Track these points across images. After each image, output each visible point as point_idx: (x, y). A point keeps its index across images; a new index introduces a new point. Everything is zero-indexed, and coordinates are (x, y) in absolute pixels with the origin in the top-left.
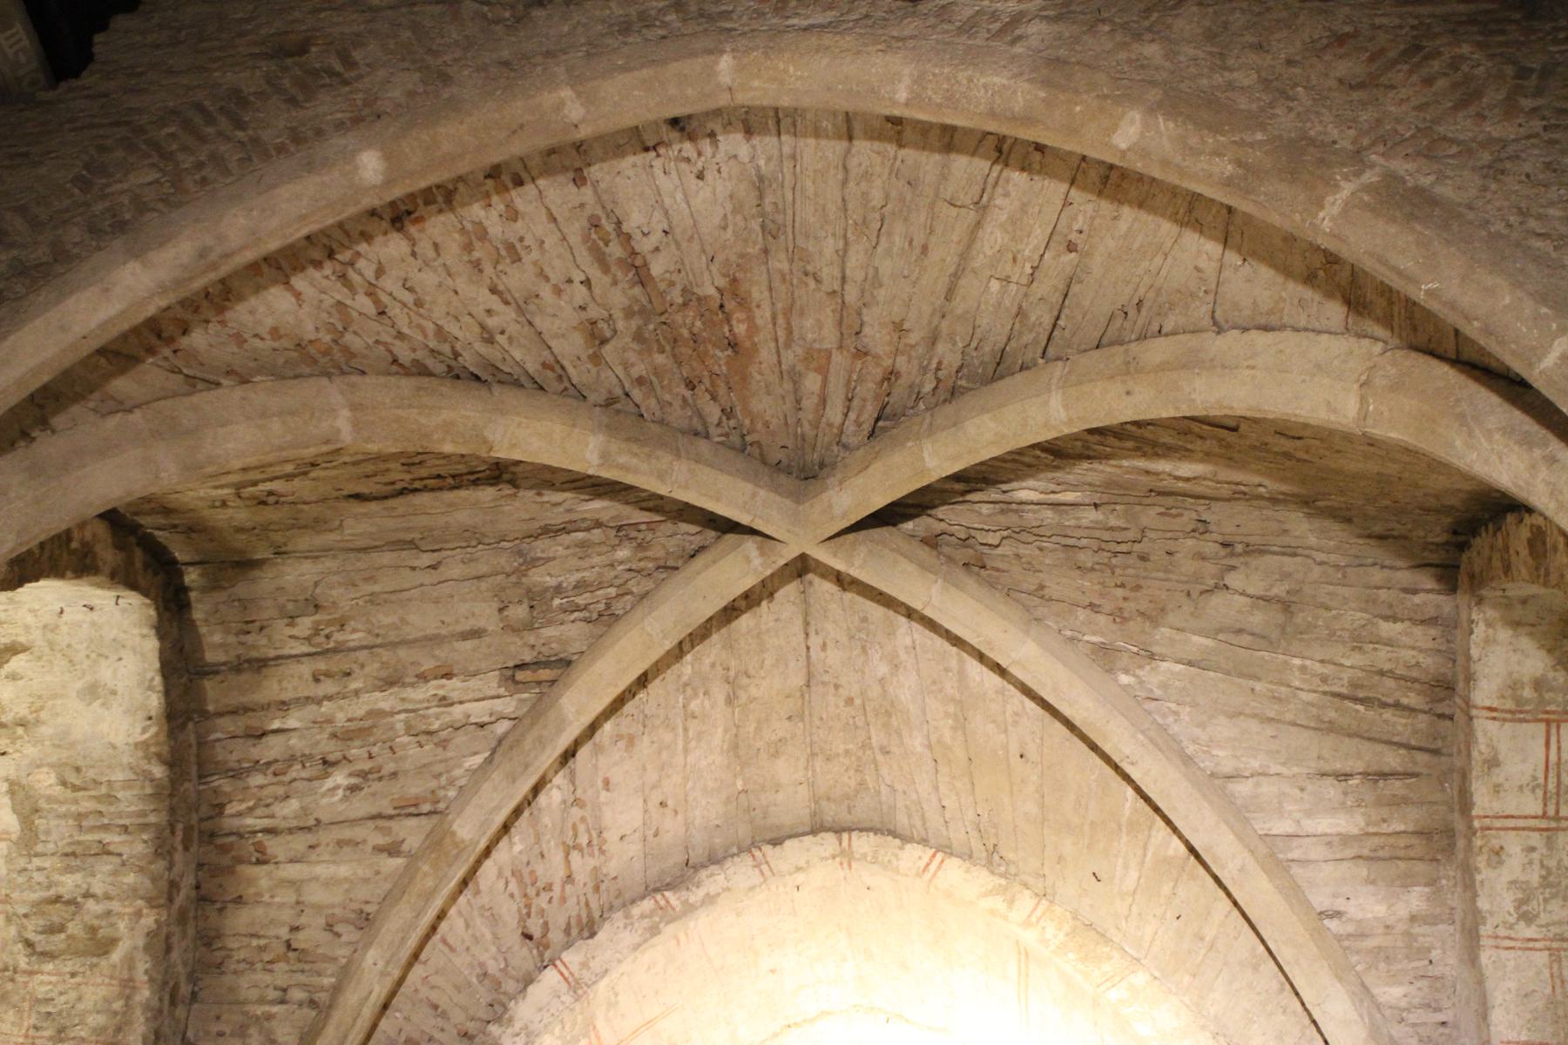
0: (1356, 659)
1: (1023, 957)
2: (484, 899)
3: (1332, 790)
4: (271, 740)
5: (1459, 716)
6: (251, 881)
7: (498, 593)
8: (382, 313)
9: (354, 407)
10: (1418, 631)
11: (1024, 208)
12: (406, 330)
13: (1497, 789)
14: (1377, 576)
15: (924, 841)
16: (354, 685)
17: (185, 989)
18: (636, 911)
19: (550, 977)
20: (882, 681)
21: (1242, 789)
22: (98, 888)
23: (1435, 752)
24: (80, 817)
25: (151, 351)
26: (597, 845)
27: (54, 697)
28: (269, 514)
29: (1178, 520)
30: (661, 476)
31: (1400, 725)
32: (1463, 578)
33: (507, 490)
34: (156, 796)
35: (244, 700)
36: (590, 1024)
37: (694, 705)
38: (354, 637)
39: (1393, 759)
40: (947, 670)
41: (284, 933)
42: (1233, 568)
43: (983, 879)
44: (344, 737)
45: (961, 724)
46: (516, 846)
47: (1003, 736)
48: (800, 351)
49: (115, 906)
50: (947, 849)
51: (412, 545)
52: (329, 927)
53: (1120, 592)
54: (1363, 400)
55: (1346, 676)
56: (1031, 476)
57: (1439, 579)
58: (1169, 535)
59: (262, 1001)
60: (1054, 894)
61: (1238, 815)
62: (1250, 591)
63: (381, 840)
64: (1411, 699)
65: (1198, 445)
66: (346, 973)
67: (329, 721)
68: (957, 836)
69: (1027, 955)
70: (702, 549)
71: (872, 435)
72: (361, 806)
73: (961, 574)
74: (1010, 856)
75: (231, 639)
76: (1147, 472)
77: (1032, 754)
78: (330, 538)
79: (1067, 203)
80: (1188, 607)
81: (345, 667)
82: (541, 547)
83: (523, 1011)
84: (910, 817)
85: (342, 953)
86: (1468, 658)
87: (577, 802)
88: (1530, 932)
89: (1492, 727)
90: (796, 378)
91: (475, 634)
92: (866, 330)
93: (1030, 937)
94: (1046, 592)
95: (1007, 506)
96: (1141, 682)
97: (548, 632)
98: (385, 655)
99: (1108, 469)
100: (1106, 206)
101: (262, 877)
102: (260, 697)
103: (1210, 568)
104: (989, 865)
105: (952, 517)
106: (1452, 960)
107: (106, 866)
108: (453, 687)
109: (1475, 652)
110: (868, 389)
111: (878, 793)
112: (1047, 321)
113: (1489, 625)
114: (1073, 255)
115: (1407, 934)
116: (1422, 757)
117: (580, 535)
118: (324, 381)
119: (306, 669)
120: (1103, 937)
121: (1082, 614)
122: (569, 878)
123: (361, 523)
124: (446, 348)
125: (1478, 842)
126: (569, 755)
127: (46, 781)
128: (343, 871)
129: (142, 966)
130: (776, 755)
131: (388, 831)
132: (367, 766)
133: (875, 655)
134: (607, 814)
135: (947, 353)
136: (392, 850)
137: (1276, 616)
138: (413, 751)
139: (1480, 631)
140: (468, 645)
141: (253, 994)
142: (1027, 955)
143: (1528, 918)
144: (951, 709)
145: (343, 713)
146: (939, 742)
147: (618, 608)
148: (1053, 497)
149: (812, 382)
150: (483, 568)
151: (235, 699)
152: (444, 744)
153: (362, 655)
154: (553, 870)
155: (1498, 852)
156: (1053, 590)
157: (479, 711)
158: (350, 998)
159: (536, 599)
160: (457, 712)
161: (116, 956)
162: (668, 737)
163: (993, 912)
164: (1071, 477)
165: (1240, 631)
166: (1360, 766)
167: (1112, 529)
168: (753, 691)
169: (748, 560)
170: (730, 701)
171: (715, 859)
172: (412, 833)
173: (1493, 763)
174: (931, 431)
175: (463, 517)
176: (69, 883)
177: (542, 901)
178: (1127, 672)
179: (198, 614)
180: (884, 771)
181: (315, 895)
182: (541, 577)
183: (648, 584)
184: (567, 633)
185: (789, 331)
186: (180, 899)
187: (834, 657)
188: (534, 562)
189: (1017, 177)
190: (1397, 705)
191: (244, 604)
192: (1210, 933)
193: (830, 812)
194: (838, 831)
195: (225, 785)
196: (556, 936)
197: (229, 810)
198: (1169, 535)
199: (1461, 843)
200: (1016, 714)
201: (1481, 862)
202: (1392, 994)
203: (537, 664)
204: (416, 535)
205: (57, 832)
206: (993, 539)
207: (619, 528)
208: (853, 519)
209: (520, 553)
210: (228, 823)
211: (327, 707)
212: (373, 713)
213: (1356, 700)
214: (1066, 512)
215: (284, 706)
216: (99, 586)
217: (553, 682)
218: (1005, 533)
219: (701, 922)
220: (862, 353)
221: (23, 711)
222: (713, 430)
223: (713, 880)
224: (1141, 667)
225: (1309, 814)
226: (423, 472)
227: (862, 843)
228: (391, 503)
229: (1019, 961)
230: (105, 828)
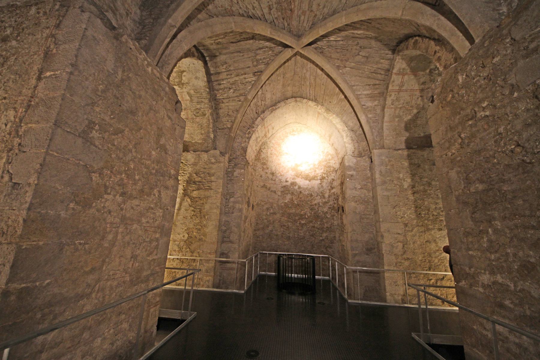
0: (376, 66)
2: (251, 108)
3: (367, 87)
4: (222, 85)
5: (390, 75)
6: (222, 106)
7: (252, 60)
8: (238, 3)
9: (235, 22)
10: (386, 61)
12: (241, 7)
13: (393, 86)
14: (383, 52)
15: (307, 99)
16: (233, 76)
17: (216, 120)
18: (269, 109)
19: (259, 118)
20: (305, 73)
21: (354, 88)
22: (202, 107)
23: (384, 81)
24: (198, 97)
25: (203, 9)
26: (265, 100)
27: (191, 79)
28: (220, 46)
30: (279, 36)
32: (396, 52)
33: (255, 41)
34: (208, 94)
35: (217, 79)
36: (264, 124)
37: (279, 78)
38: (232, 68)
41: (227, 113)
42: (361, 51)
43: (314, 103)
44: (232, 84)
45: (315, 79)
46: (255, 100)
48: (301, 11)
49: (205, 109)
50: (310, 100)
51: (240, 52)
52: (233, 112)
54: (403, 12)
55: (374, 69)
56: (334, 35)
57: (392, 52)
59: (225, 122)
61: (353, 91)
63: (238, 99)
64: (383, 73)
65: (363, 27)
66: (236, 118)
67: (229, 82)
68: (311, 97)
70: (282, 51)
71: (310, 28)
72: (235, 95)
73: (319, 54)
74: (318, 100)
75: (214, 69)
76: (353, 33)
77: (324, 84)
78: (228, 51)
81: (231, 73)
82: (259, 52)
83: (256, 122)
85: (235, 115)
86: (394, 65)
87: (263, 94)
88: (393, 106)
90: (300, 17)
91: (249, 67)
92: (313, 6)
93: (320, 111)
95: (328, 41)
97: (259, 67)
98: (237, 71)
101: (223, 105)
102: (219, 78)
104: (315, 101)
106: (379, 111)
107: (203, 104)
108: (246, 76)
109: (395, 64)
110: (311, 19)
113: (399, 59)
115: (374, 108)
116: (382, 82)
117: (264, 49)
118: (229, 17)
119: (225, 74)
120: (330, 111)
121: (336, 60)
122: (262, 105)
123: (232, 48)
124: (247, 11)
125: (388, 94)
126: (262, 86)
127: (192, 92)
128: (234, 104)
129: (210, 117)
130: (288, 86)
131: (239, 98)
132: (235, 89)
133: (304, 69)
134: (266, 95)
135: (326, 10)
136: (240, 101)
137: (365, 59)
138: (241, 86)
139: (397, 60)
140: (248, 69)
141: (224, 121)
143: (393, 104)
145: (231, 81)
147: (269, 62)
148: (336, 39)
149: (302, 18)
150: (250, 56)
151: (216, 79)
152: (245, 85)
153: (233, 71)
154: (259, 104)
155: (391, 95)
156: (333, 57)
157: (250, 80)
158: (237, 121)
159: (257, 61)
160: (247, 80)
161: (207, 116)
162: (275, 83)
163: (315, 108)
165: (359, 62)
168: (287, 76)
169: (289, 52)
170: (283, 77)
171: (279, 102)
172: (242, 98)
173: (393, 82)
174: (321, 26)
175: (248, 46)
176: (198, 106)
177: (258, 108)
179: (209, 65)
181: (230, 107)
182: (258, 57)
183: (273, 58)
184: (262, 67)
185: (300, 6)
186: (214, 108)
187: (298, 70)
188: (257, 54)
190: (380, 74)
191: (216, 63)
192: (345, 109)
193: (295, 95)
194: (295, 97)
195: (216, 92)
196: (260, 113)
197: (218, 96)
199: (385, 94)
201: (388, 97)
202: (370, 116)
203: (258, 72)
204: (240, 50)
205: (196, 100)
206: (325, 47)
207: (270, 48)
208: (306, 44)
209: (255, 53)
210: (218, 98)
211: (229, 80)
212: (236, 81)
215: (223, 80)
216: (195, 59)
217: (260, 75)
219: (278, 111)
220: (312, 11)
221: (187, 81)
222: (286, 28)
223: (279, 105)
225: (364, 91)
226: (242, 37)
227: (298, 99)
228: (237, 44)
230: (202, 98)
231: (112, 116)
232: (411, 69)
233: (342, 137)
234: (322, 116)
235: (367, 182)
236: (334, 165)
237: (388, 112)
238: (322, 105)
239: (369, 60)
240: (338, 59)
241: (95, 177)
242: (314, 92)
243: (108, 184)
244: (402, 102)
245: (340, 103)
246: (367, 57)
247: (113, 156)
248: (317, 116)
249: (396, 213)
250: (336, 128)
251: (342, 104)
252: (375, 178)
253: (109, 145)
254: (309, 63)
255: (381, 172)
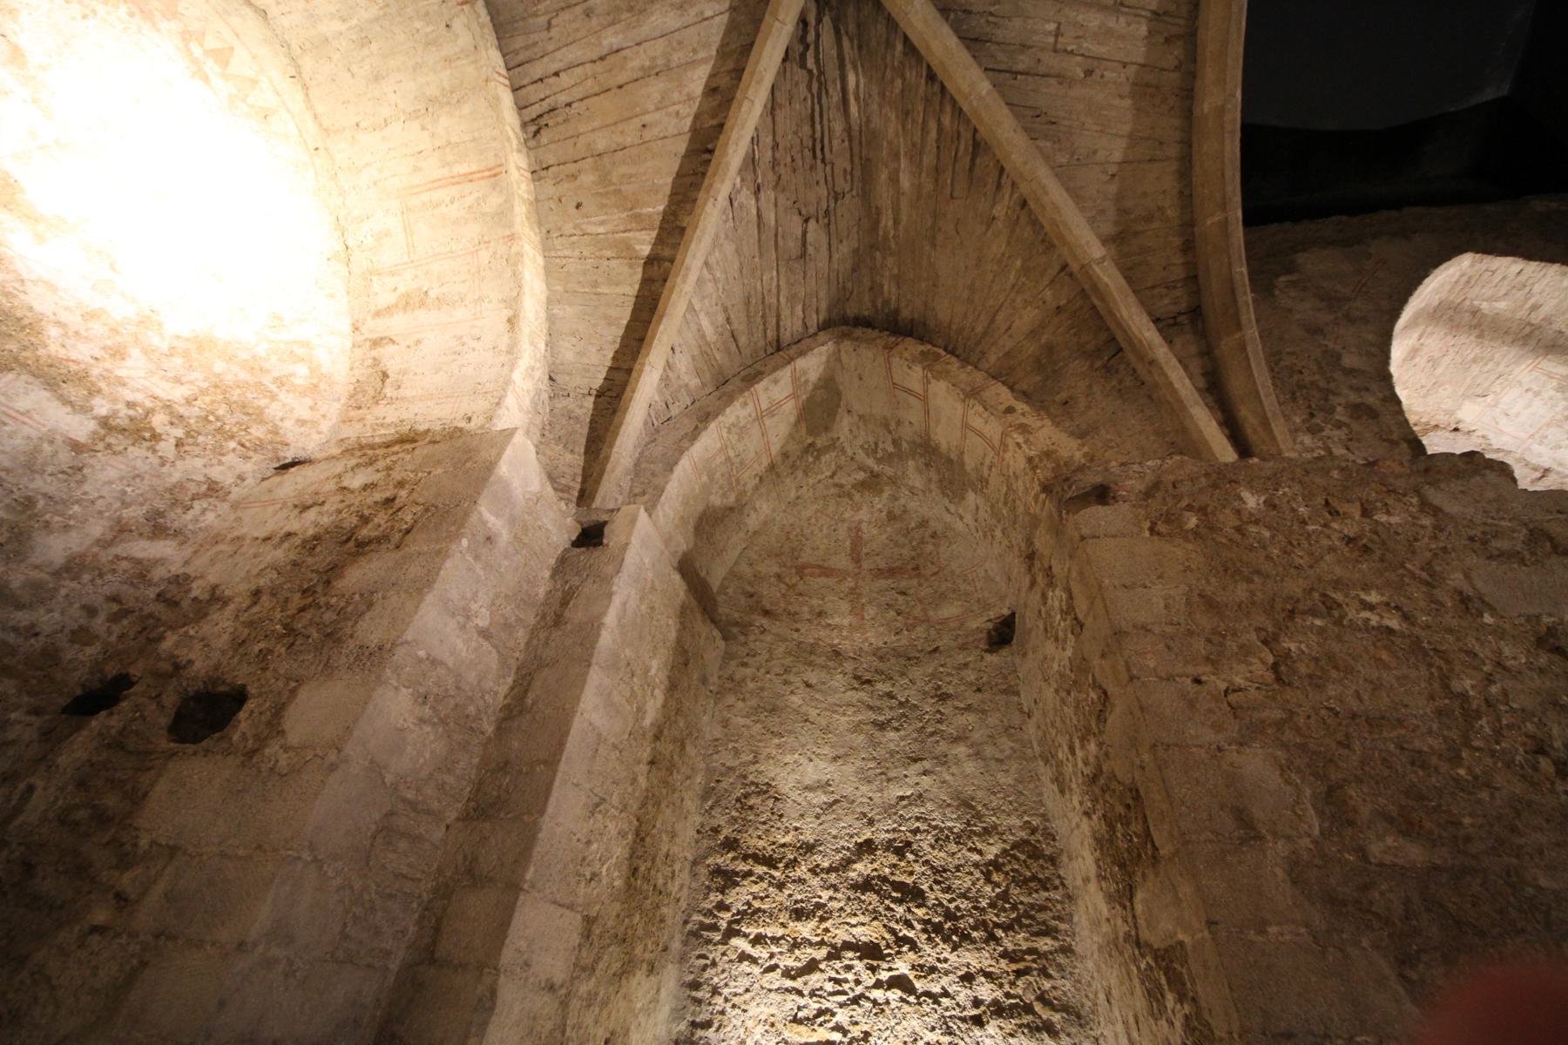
1: (488, 173)
3: (721, 318)
10: (800, 322)
11: (1122, 37)
14: (822, 294)
29: (842, 181)
31: (758, 334)
39: (743, 340)
40: (695, 51)
47: (653, 108)
53: (789, 160)
58: (829, 179)
60: (540, 179)
62: (808, 235)
69: (495, 175)
74: (544, 137)
77: (648, 135)
79: (1125, 65)
80: (790, 203)
84: (527, 48)
88: (725, 435)
89: (789, 374)
94: (778, 112)
96: (739, 192)
99: (891, 131)
100: (1126, 89)
103: (812, 210)
104: (524, 125)
105: (826, 28)
109: (815, 351)
111: (535, 15)
112: (1021, 67)
114: (1082, 75)
121: (769, 140)
125: (746, 394)
142: (495, 175)
143: (729, 431)
144: (660, 62)
146: (625, 58)
155: (746, 404)
163: (509, 139)
164: (875, 107)
166: (735, 326)
167: (830, 142)
178: (743, 180)
180: (565, 16)
189: (1143, 29)
192: (603, 289)
198: (829, 179)
200: (678, 113)
206: (811, 64)
213: (764, 310)
214: (838, 109)
218: (815, 71)
224: (748, 189)
225: (707, 313)
229: (479, 172)
232: (808, 399)
233: (512, 350)
234: (495, 200)
235: (519, 620)
236: (288, 424)
237: (710, 440)
238: (538, 172)
239: (797, 266)
240: (775, 146)
242: (578, 93)
244: (740, 447)
245: (609, 253)
246: (803, 254)
248: (463, 169)
249: (589, 843)
250: (513, 304)
251: (613, 263)
252: (592, 628)
254: (727, 5)
255: (624, 604)
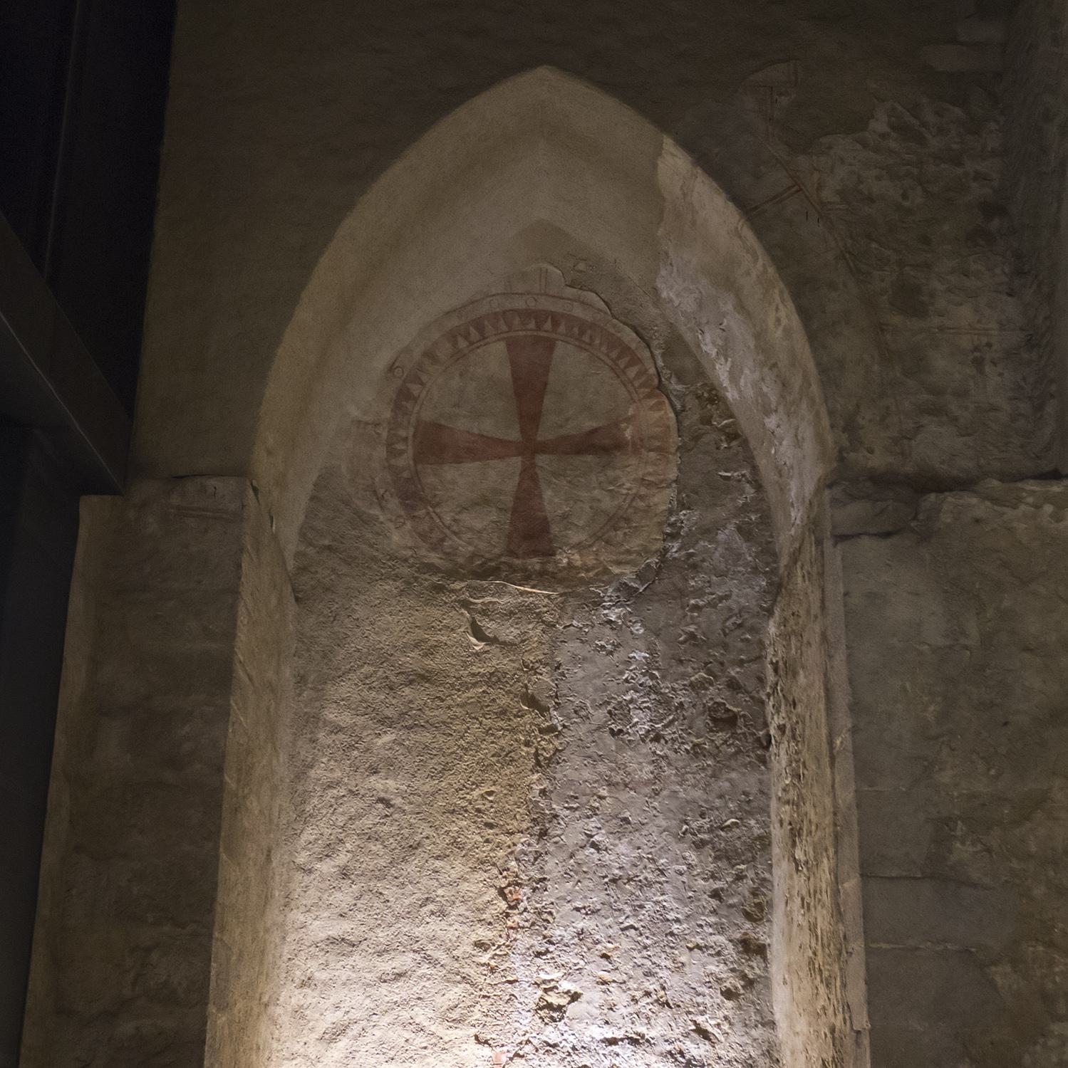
231: (992, 772)
241: (1002, 975)
243: (1050, 986)
247: (1039, 891)
253: (1015, 864)
